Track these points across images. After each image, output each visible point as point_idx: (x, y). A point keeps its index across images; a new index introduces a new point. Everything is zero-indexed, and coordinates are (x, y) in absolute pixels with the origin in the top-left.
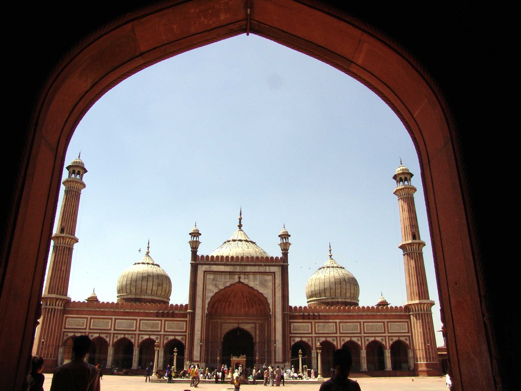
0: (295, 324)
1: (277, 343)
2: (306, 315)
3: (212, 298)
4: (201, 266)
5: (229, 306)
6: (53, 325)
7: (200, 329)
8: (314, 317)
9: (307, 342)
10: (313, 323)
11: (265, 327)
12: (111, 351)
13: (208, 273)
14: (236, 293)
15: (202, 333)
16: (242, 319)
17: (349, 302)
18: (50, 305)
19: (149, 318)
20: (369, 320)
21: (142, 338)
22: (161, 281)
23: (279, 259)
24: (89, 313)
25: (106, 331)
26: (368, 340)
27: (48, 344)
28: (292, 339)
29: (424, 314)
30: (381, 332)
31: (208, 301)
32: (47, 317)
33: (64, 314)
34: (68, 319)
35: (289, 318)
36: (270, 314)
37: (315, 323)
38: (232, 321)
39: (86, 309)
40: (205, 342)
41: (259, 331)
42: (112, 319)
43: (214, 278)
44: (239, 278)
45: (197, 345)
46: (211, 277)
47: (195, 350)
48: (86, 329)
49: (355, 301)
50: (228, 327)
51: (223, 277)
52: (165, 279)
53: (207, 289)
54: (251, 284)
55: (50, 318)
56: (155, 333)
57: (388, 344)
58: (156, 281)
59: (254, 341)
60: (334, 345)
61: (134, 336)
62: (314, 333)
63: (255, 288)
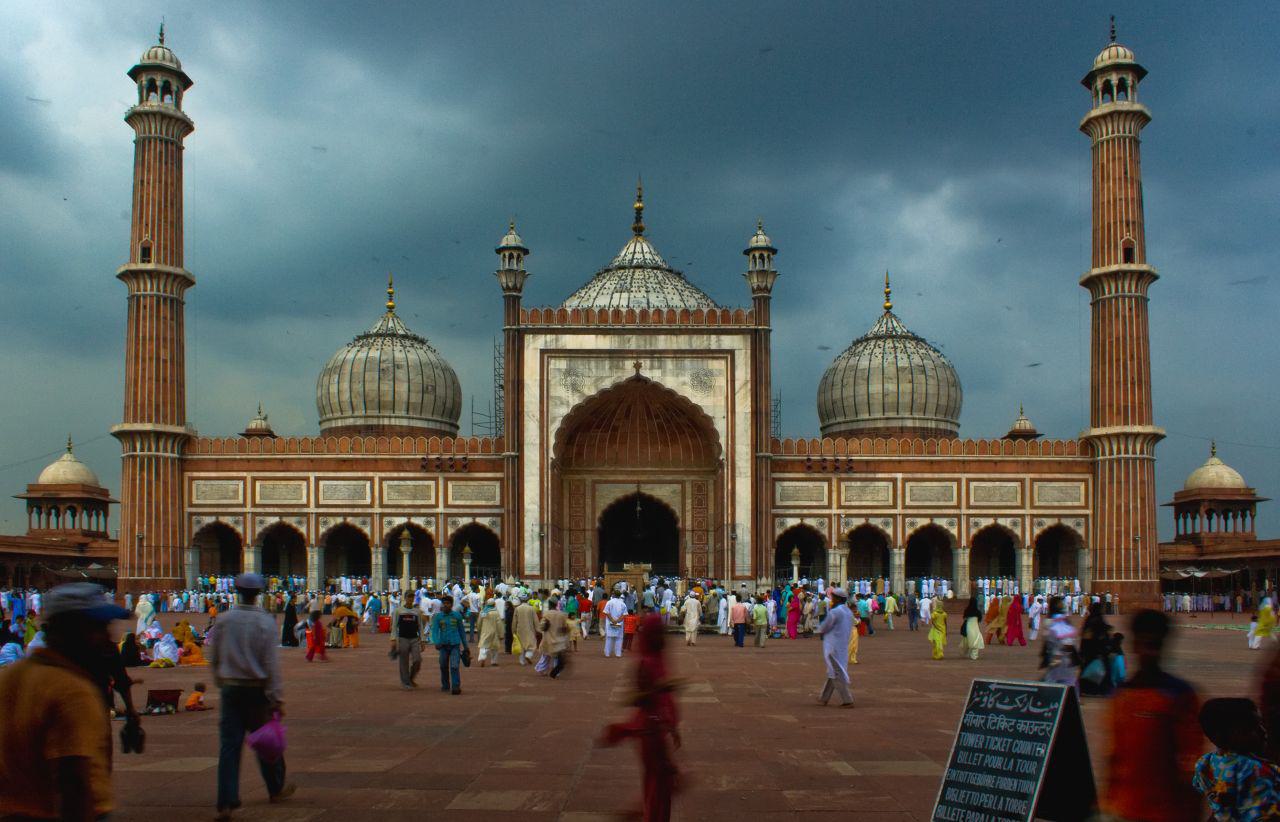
0: (786, 484)
1: (739, 531)
2: (818, 461)
3: (567, 419)
6: (157, 498)
7: (537, 499)
8: (837, 467)
10: (834, 483)
12: (313, 557)
17: (931, 429)
18: (142, 450)
19: (402, 475)
20: (985, 476)
21: (390, 523)
24: (249, 465)
25: (296, 510)
26: (976, 524)
27: (153, 544)
28: (777, 520)
29: (1135, 459)
30: (1014, 504)
31: (554, 427)
32: (142, 479)
33: (182, 471)
34: (195, 484)
35: (771, 468)
36: (721, 458)
37: (840, 480)
38: (621, 478)
39: (238, 457)
40: (553, 531)
42: (307, 479)
44: (638, 366)
45: (533, 538)
46: (562, 364)
48: (244, 505)
49: (949, 427)
50: (610, 494)
51: (593, 363)
52: (442, 375)
53: (552, 397)
54: (670, 382)
55: (150, 483)
56: (423, 511)
57: (1028, 534)
58: (417, 379)
59: (680, 525)
60: (888, 536)
61: (368, 519)
62: (835, 505)
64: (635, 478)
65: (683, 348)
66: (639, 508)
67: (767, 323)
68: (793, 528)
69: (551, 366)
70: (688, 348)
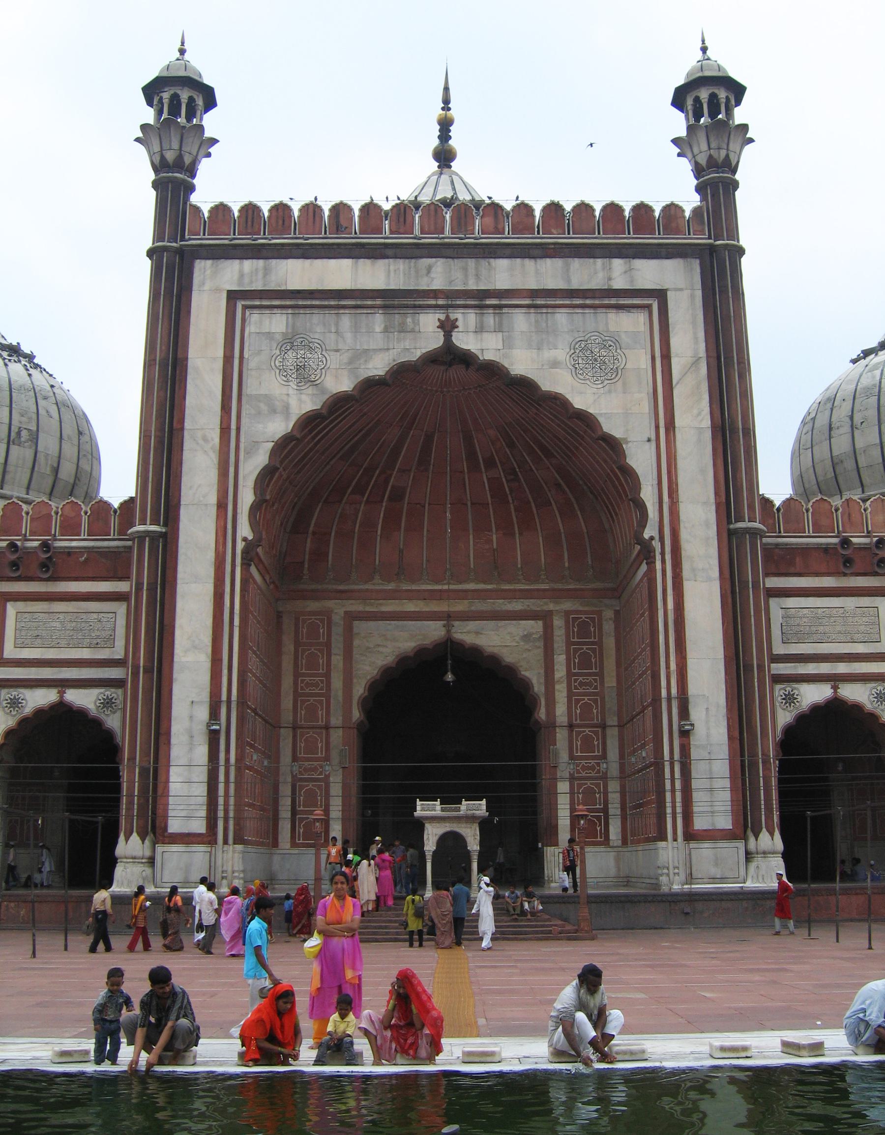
0: (792, 602)
1: (697, 714)
4: (209, 262)
5: (392, 520)
9: (869, 706)
11: (601, 637)
13: (257, 303)
14: (429, 438)
15: (221, 660)
16: (466, 591)
22: (24, 419)
23: (687, 214)
36: (646, 536)
38: (410, 607)
40: (241, 719)
41: (568, 660)
43: (295, 334)
44: (447, 327)
45: (192, 737)
47: (173, 770)
51: (346, 321)
52: (55, 414)
59: (542, 714)
63: (546, 386)
64: (442, 607)
65: (552, 284)
66: (450, 677)
67: (733, 232)
68: (817, 710)
69: (250, 329)
70: (562, 285)
